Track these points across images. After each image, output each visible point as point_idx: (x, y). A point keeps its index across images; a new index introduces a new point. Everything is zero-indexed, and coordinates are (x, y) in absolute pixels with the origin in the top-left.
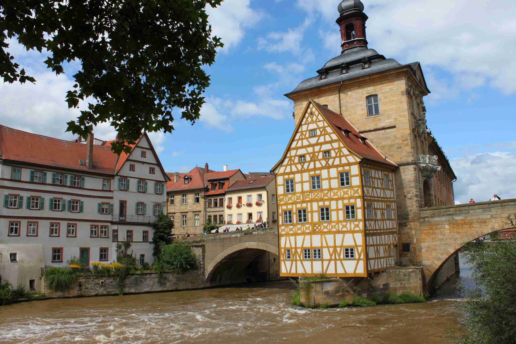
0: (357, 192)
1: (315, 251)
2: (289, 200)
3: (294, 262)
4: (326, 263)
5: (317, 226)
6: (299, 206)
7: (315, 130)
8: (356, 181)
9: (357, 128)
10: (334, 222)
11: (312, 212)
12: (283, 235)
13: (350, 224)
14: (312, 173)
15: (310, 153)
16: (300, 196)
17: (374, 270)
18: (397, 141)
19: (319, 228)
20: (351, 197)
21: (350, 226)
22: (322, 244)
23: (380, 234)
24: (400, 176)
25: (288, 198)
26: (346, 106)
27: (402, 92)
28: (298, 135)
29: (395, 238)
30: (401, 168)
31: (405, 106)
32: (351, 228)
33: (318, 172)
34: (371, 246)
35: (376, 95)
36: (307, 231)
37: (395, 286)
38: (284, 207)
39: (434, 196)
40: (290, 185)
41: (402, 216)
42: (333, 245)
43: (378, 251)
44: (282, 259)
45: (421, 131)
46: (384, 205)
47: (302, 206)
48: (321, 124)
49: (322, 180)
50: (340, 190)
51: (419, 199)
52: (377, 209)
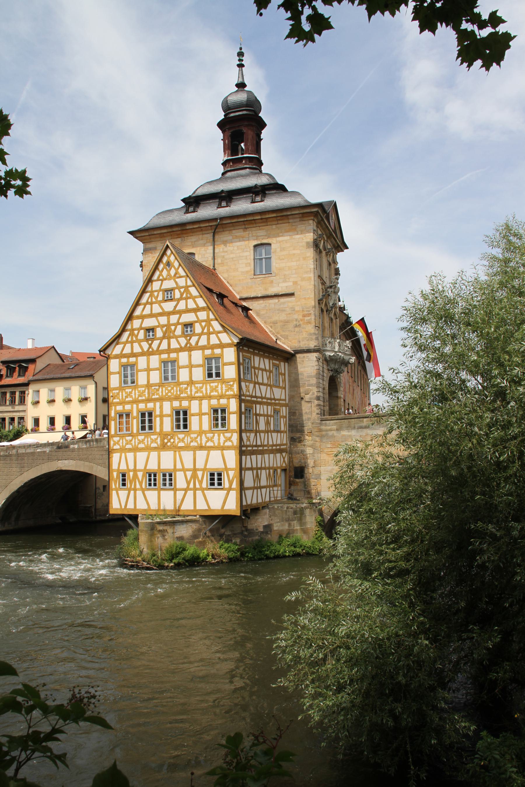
0: (231, 388)
1: (164, 475)
2: (126, 397)
3: (132, 492)
4: (180, 494)
5: (169, 437)
6: (142, 406)
7: (171, 290)
8: (230, 372)
9: (237, 292)
10: (194, 432)
11: (162, 416)
12: (116, 451)
13: (219, 436)
14: (164, 356)
15: (163, 326)
16: (144, 391)
17: (251, 505)
18: (296, 316)
19: (172, 440)
20: (221, 397)
21: (219, 439)
22: (175, 465)
23: (262, 453)
24: (296, 368)
25: (126, 393)
26: (223, 257)
27: (308, 243)
28: (146, 296)
29: (284, 458)
30: (298, 356)
31: (311, 264)
32: (219, 443)
33: (173, 355)
34: (249, 469)
35: (269, 244)
36: (154, 445)
37: (281, 528)
38: (119, 408)
39: (342, 400)
40: (129, 372)
41: (296, 427)
42: (192, 467)
43: (257, 478)
44: (114, 487)
45: (331, 304)
46: (270, 410)
47: (146, 406)
48: (182, 282)
49: (179, 368)
50: (206, 383)
51: (322, 403)
52: (260, 415)
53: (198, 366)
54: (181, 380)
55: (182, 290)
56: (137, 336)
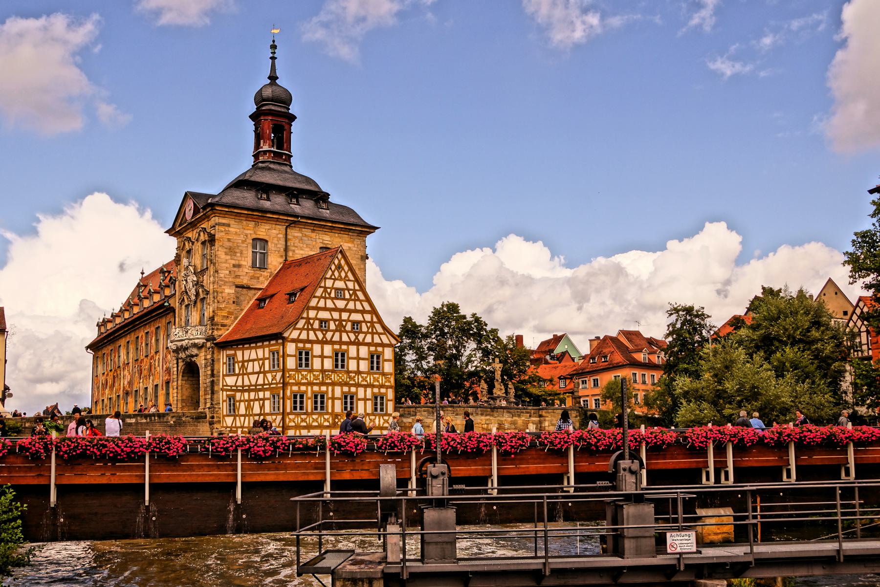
11: (333, 399)
14: (337, 347)
20: (382, 386)
26: (294, 251)
33: (344, 347)
38: (295, 388)
40: (304, 357)
49: (349, 358)
53: (363, 359)
54: (350, 369)
55: (351, 292)
56: (312, 325)
